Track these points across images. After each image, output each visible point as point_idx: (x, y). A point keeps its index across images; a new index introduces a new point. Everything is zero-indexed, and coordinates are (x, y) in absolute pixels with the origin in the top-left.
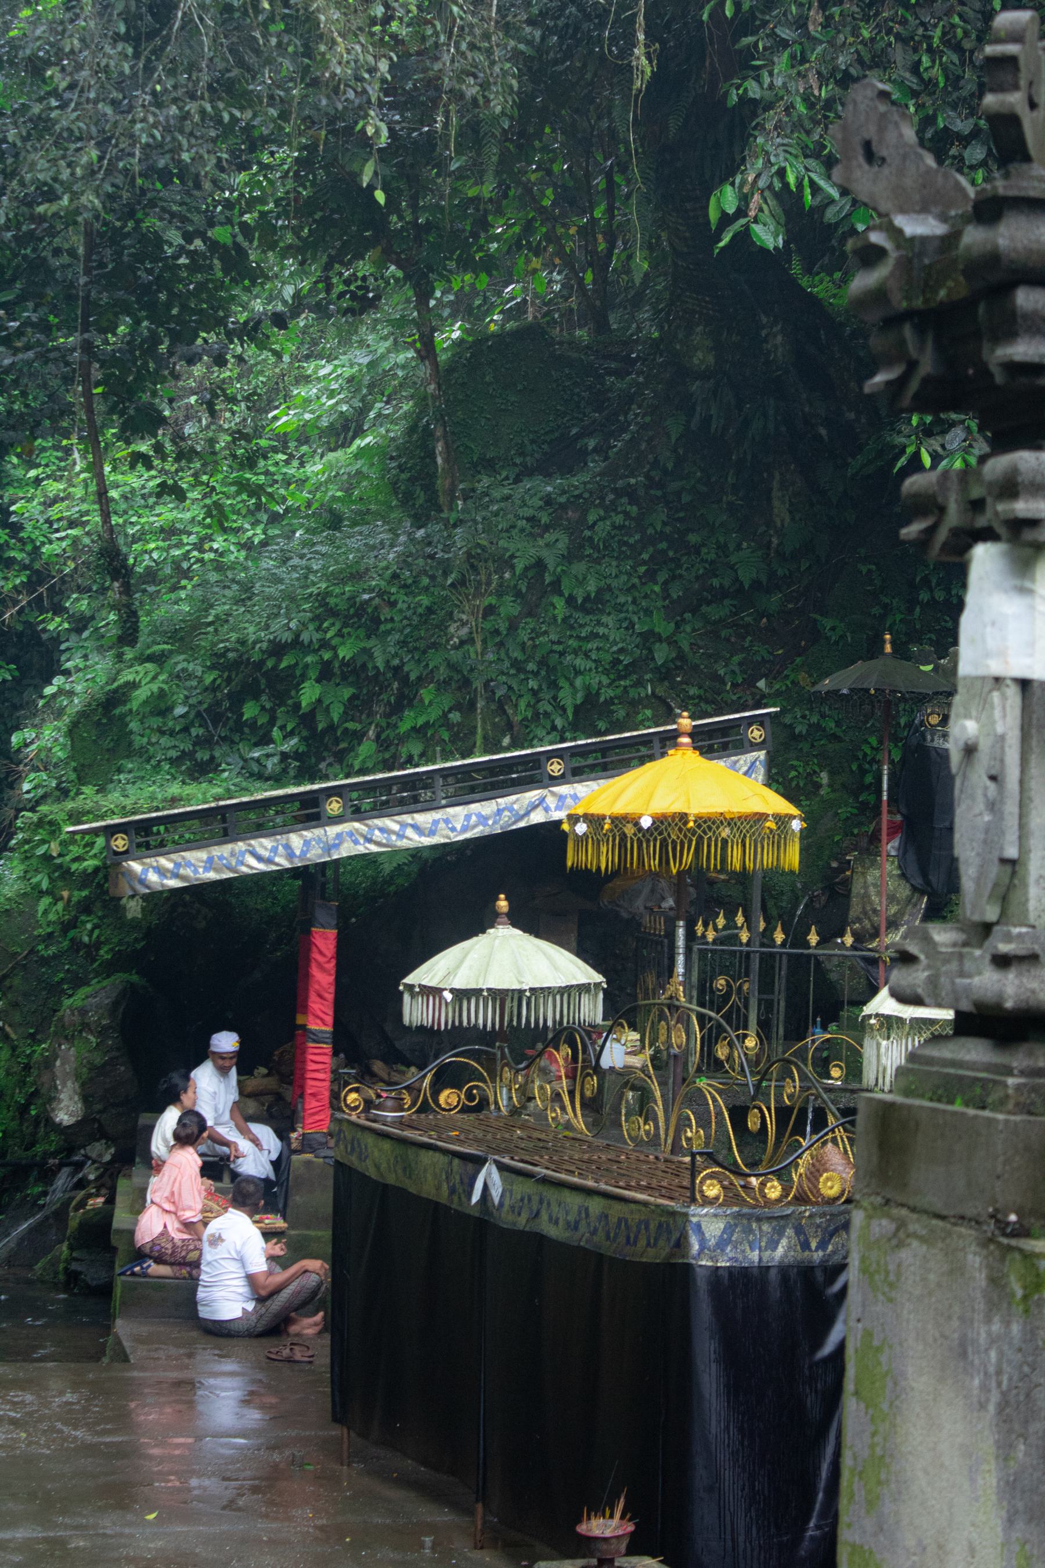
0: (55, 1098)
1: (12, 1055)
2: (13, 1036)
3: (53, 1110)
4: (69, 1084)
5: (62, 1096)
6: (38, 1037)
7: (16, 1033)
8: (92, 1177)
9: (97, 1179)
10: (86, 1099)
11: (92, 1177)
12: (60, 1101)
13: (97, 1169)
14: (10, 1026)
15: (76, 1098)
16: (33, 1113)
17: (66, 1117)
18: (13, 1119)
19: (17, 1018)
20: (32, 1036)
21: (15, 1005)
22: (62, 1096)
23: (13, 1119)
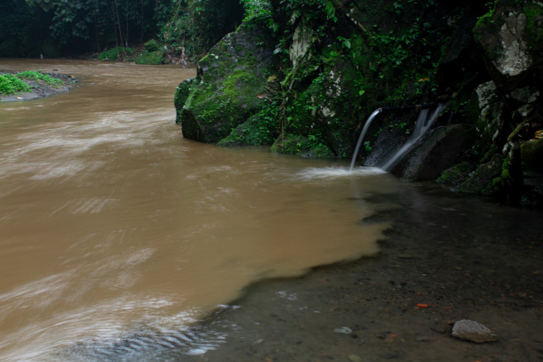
0: (500, 55)
1: (365, 42)
2: (364, 30)
3: (499, 64)
4: (515, 43)
5: (507, 53)
6: (379, 30)
7: (365, 28)
8: (524, 114)
9: (529, 115)
10: (529, 52)
11: (524, 114)
12: (505, 57)
13: (528, 108)
14: (361, 23)
15: (522, 54)
16: (382, 77)
17: (512, 69)
18: (369, 81)
19: (365, 18)
20: (375, 29)
21: (364, 10)
22: (507, 53)
23: (369, 81)
